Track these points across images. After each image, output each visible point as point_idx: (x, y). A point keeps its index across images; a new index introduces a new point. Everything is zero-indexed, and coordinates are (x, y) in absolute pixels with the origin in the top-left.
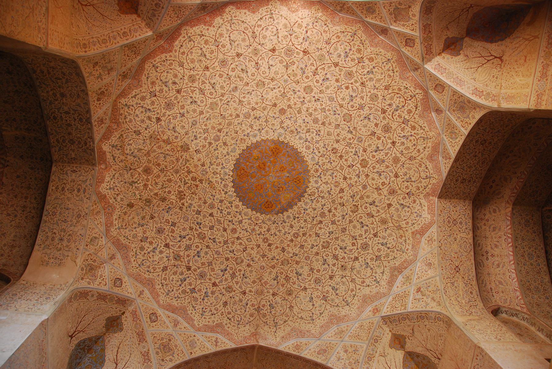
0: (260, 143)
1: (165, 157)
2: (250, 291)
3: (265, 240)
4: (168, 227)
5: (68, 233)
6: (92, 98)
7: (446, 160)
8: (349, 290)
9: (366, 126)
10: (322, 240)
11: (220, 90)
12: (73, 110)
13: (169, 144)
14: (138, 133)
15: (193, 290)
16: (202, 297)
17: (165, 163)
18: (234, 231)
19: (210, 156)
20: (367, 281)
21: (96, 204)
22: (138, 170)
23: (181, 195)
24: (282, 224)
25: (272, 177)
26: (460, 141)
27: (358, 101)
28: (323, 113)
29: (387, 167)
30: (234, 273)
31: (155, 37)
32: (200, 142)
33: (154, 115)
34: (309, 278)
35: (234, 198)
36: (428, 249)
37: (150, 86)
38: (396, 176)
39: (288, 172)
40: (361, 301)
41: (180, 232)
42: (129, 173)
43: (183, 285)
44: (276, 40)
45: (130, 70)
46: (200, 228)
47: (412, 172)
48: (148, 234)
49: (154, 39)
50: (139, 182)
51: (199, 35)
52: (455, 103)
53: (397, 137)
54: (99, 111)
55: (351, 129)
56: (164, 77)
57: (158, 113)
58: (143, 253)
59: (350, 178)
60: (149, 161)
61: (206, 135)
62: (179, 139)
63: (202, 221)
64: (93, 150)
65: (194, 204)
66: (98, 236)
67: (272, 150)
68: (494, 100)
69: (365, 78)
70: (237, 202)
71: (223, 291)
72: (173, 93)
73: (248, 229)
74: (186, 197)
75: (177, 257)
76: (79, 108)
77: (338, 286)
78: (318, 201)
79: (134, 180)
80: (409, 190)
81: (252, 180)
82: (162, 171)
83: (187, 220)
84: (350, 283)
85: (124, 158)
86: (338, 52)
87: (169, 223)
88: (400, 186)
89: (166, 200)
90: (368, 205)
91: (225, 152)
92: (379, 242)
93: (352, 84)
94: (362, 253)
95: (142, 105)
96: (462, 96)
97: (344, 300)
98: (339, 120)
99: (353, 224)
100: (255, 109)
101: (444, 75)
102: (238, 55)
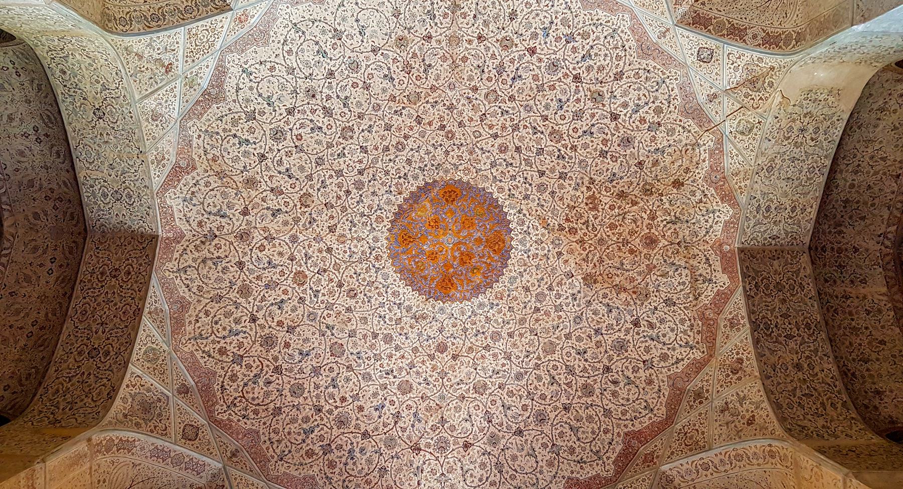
0: (472, 296)
1: (622, 264)
2: (470, 42)
3: (450, 136)
4: (612, 149)
5: (790, 141)
6: (751, 364)
7: (156, 309)
8: (297, 53)
9: (304, 341)
10: (355, 141)
11: (543, 374)
12: (781, 343)
13: (617, 285)
14: (669, 302)
15: (570, 39)
16: (554, 27)
17: (621, 254)
18: (503, 149)
19: (549, 269)
20: (264, 71)
21: (740, 188)
22: (666, 243)
23: (593, 203)
24: (426, 166)
25: (448, 240)
26: (139, 350)
27: (323, 381)
28: (378, 352)
29: (258, 278)
30: (500, 74)
31: (655, 460)
32: (566, 290)
33: (643, 331)
34: (369, 70)
35: (507, 203)
36: (164, 145)
37: (654, 377)
38: (240, 264)
39: (422, 252)
40: (272, 33)
41: (592, 141)
42: (681, 237)
43: (588, 47)
44: (464, 462)
45: (691, 407)
46: (559, 150)
47: (213, 275)
48: (648, 136)
49: (658, 457)
50: (665, 223)
51: (585, 463)
52: (160, 415)
53: (248, 330)
54: (738, 341)
55: (329, 333)
56: (633, 392)
57: (638, 334)
58: (657, 103)
59: (320, 251)
60: (648, 257)
61: (559, 301)
62: (601, 293)
63: (556, 162)
64: (744, 276)
65: (571, 189)
66: (738, 136)
67: (452, 284)
68: (98, 445)
69: (316, 420)
70: (501, 197)
71: (517, 41)
72: (617, 366)
73: (480, 152)
74: (585, 201)
75: (597, 97)
76: (771, 346)
77: (317, 59)
78: (370, 207)
79: (673, 227)
80: (213, 243)
81: (479, 234)
82: (626, 242)
83: (581, 162)
84: (295, 65)
85: (691, 262)
86: (365, 457)
87: (612, 156)
88: (232, 248)
89: (617, 195)
90: (284, 209)
91: (526, 277)
92: (254, 146)
93: (336, 407)
94: (282, 123)
95: (665, 348)
96: (152, 431)
97: (303, 33)
98: (350, 345)
99: (306, 174)
100: (484, 348)
101: (187, 460)
102: (519, 432)
